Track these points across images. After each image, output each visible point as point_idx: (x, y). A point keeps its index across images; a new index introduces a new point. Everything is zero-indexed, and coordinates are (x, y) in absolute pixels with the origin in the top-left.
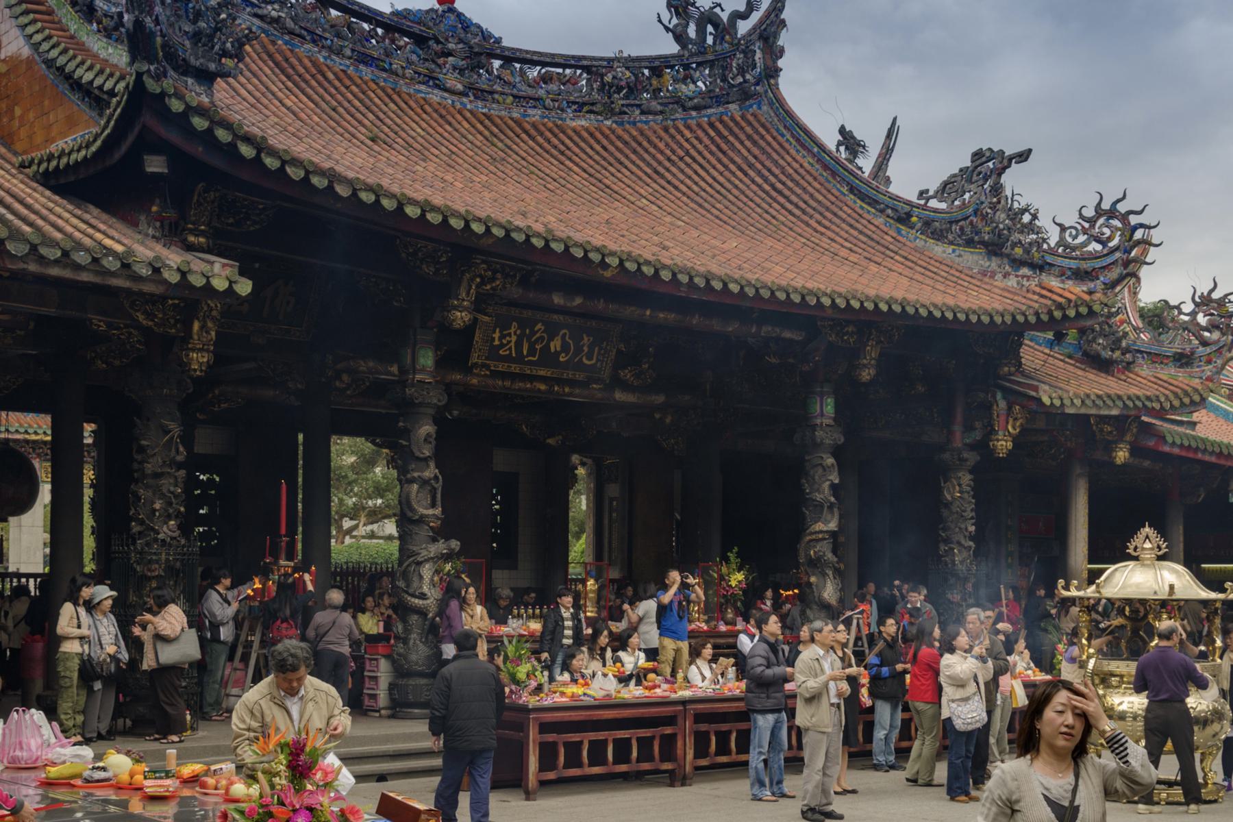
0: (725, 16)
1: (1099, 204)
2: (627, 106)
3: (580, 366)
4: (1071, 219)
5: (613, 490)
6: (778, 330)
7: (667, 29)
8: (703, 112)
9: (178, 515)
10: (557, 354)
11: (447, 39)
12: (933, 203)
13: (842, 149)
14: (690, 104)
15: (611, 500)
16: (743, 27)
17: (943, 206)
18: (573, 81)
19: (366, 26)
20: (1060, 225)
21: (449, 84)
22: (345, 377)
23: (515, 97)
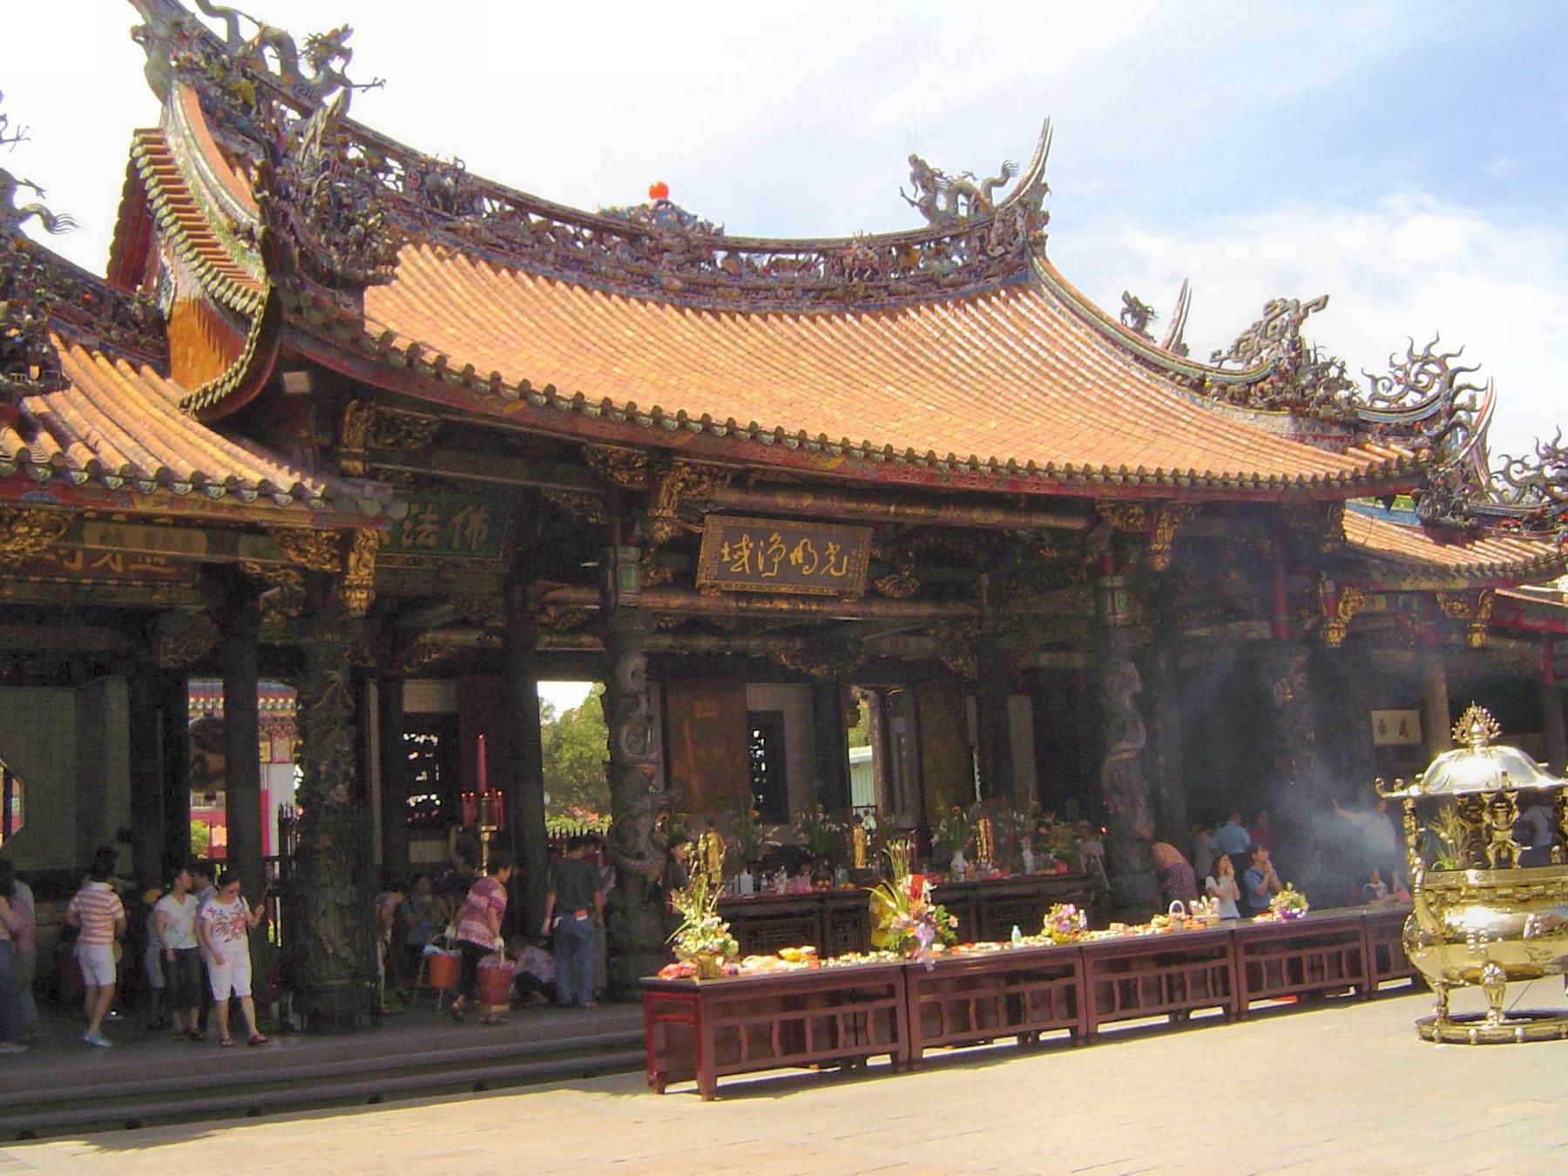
0: (978, 185)
1: (1411, 351)
4: (1382, 370)
5: (900, 724)
7: (912, 203)
8: (962, 289)
9: (346, 776)
10: (799, 566)
12: (1228, 365)
13: (1128, 317)
14: (945, 281)
15: (899, 736)
16: (999, 196)
17: (1239, 367)
18: (807, 266)
19: (570, 228)
20: (1371, 377)
21: (665, 281)
22: (552, 612)
23: (742, 289)
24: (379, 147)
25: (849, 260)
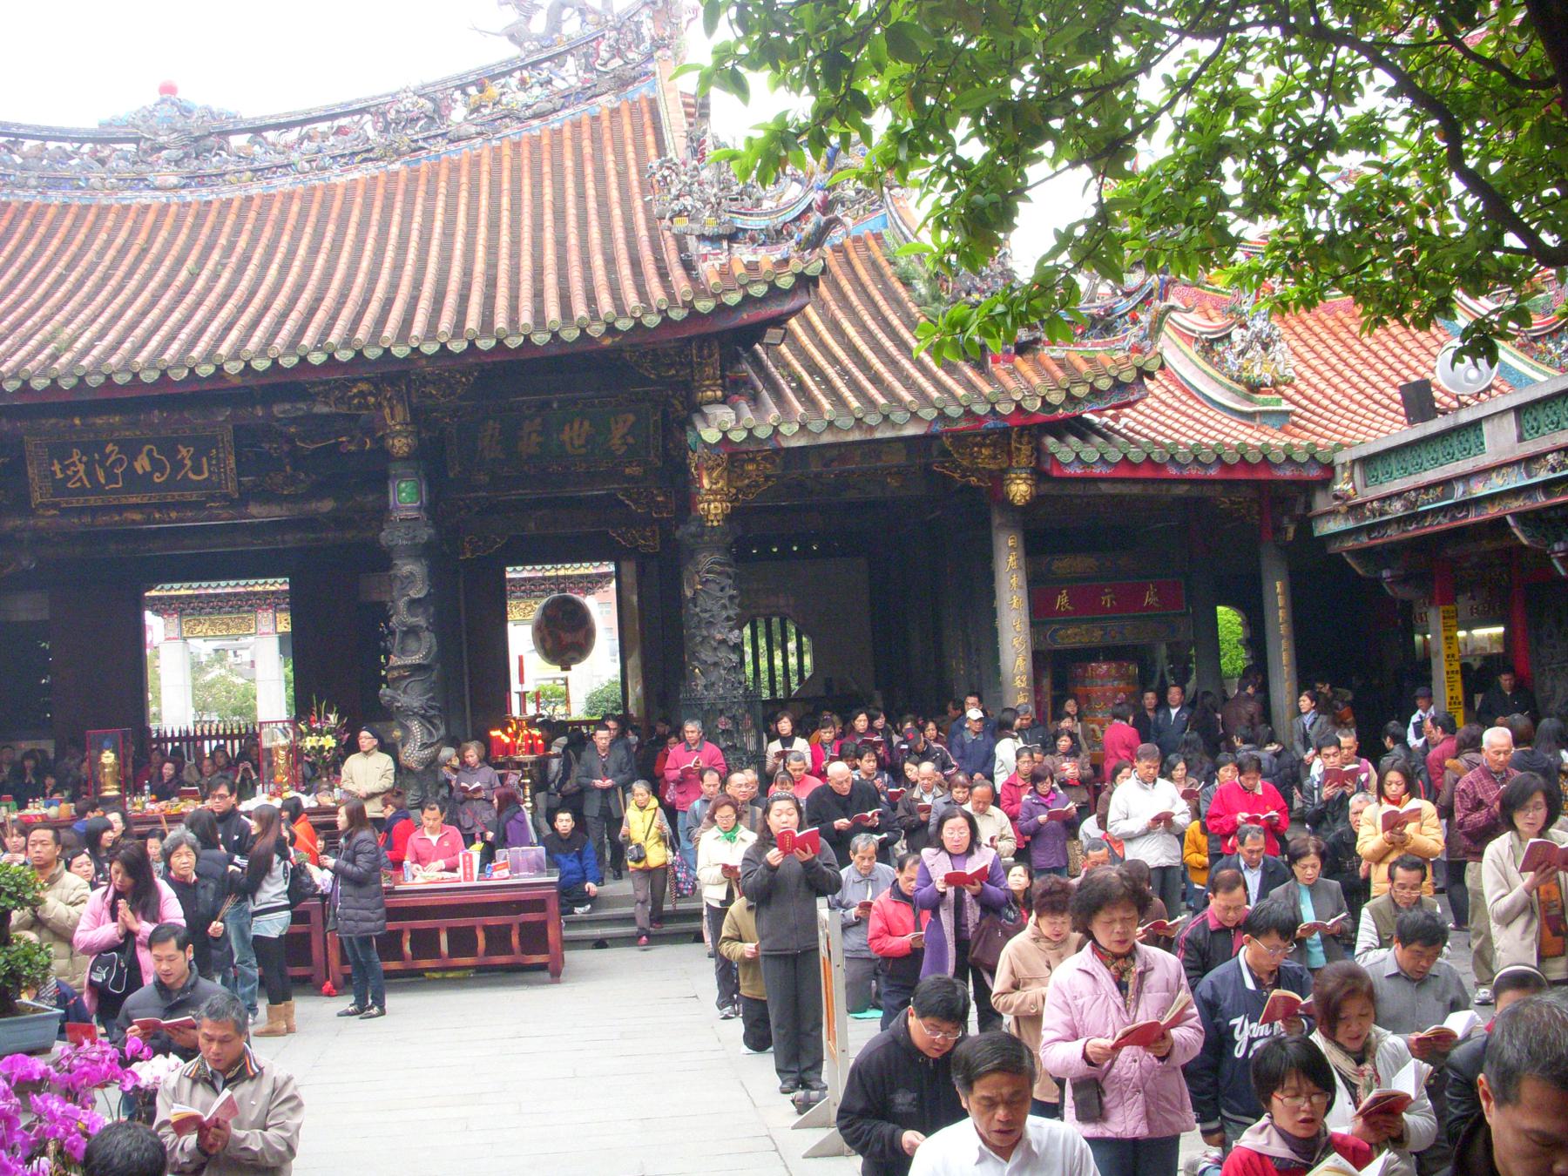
2: (425, 139)
3: (186, 484)
6: (302, 406)
11: (156, 134)
14: (528, 113)
23: (255, 171)
25: (392, 115)
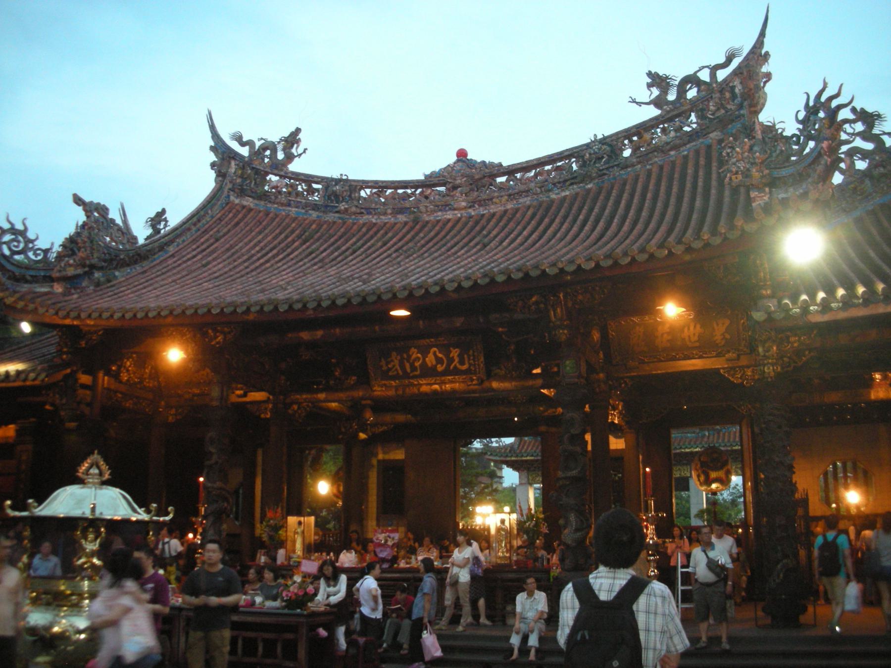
2: (607, 169)
14: (668, 147)
16: (721, 75)
23: (510, 195)
24: (309, 179)
